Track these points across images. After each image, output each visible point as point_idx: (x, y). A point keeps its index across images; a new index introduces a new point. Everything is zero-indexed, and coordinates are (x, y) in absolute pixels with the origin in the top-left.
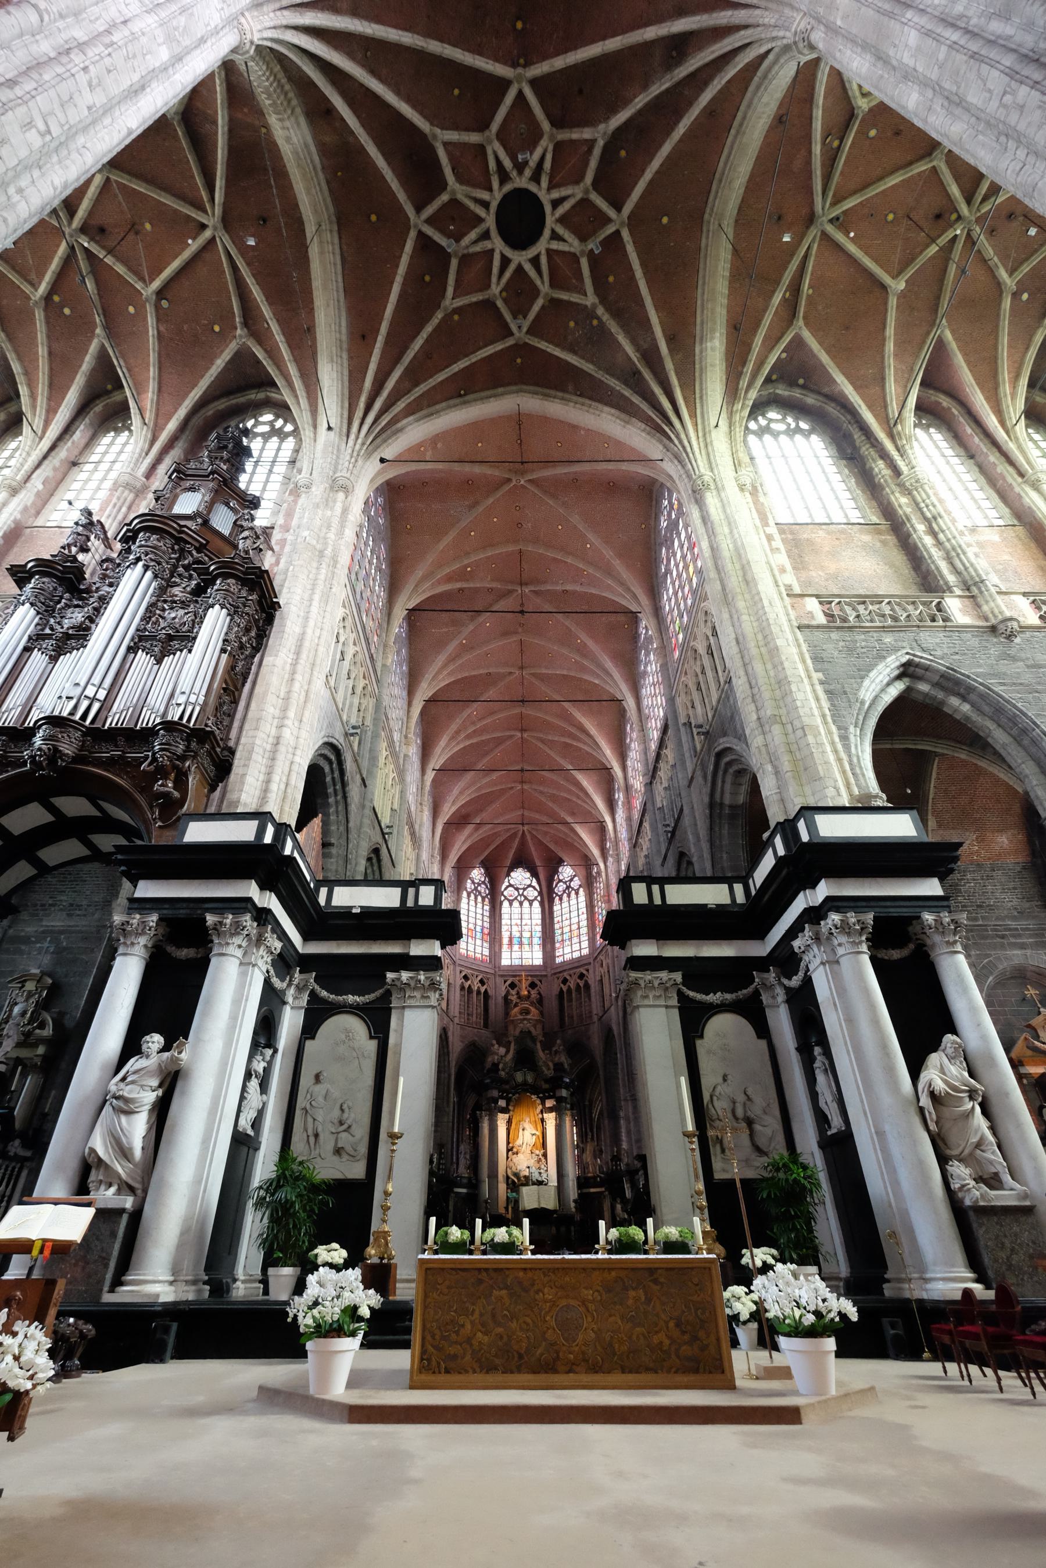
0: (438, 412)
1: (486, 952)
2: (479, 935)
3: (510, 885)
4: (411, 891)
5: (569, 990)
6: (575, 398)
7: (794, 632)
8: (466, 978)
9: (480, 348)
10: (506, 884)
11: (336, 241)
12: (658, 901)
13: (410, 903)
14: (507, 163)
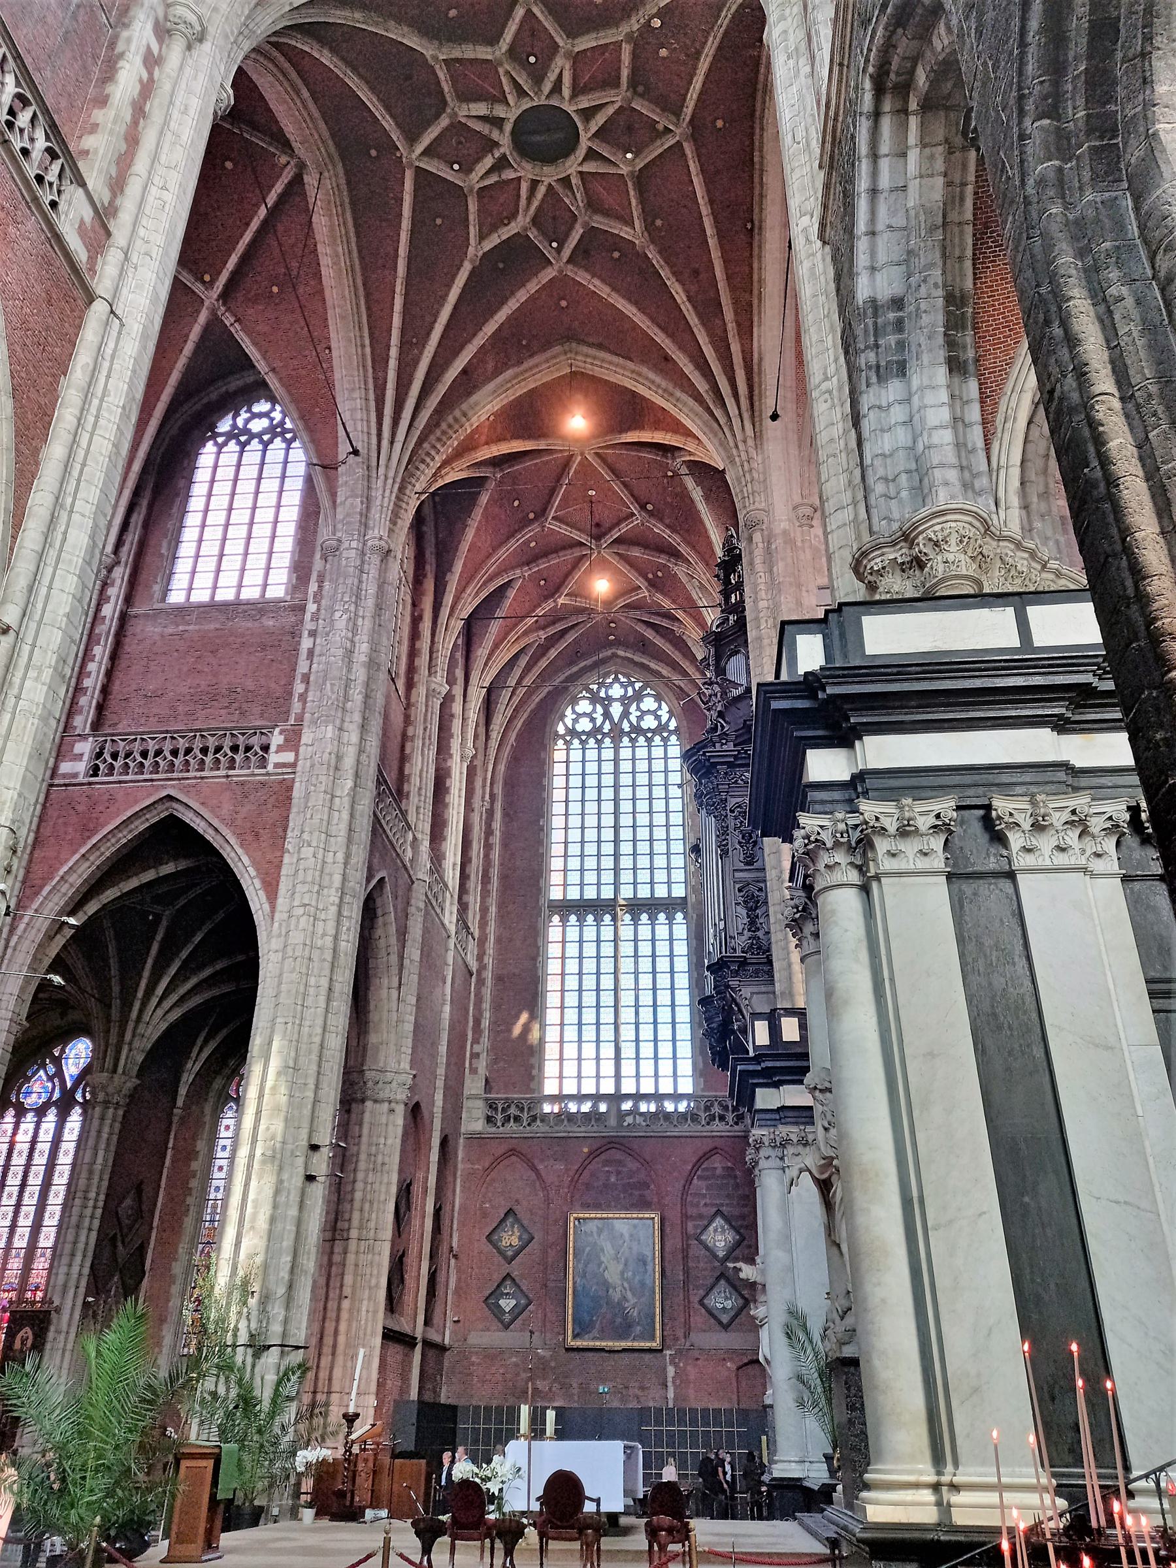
0: (760, 281)
11: (585, 349)
14: (488, 162)
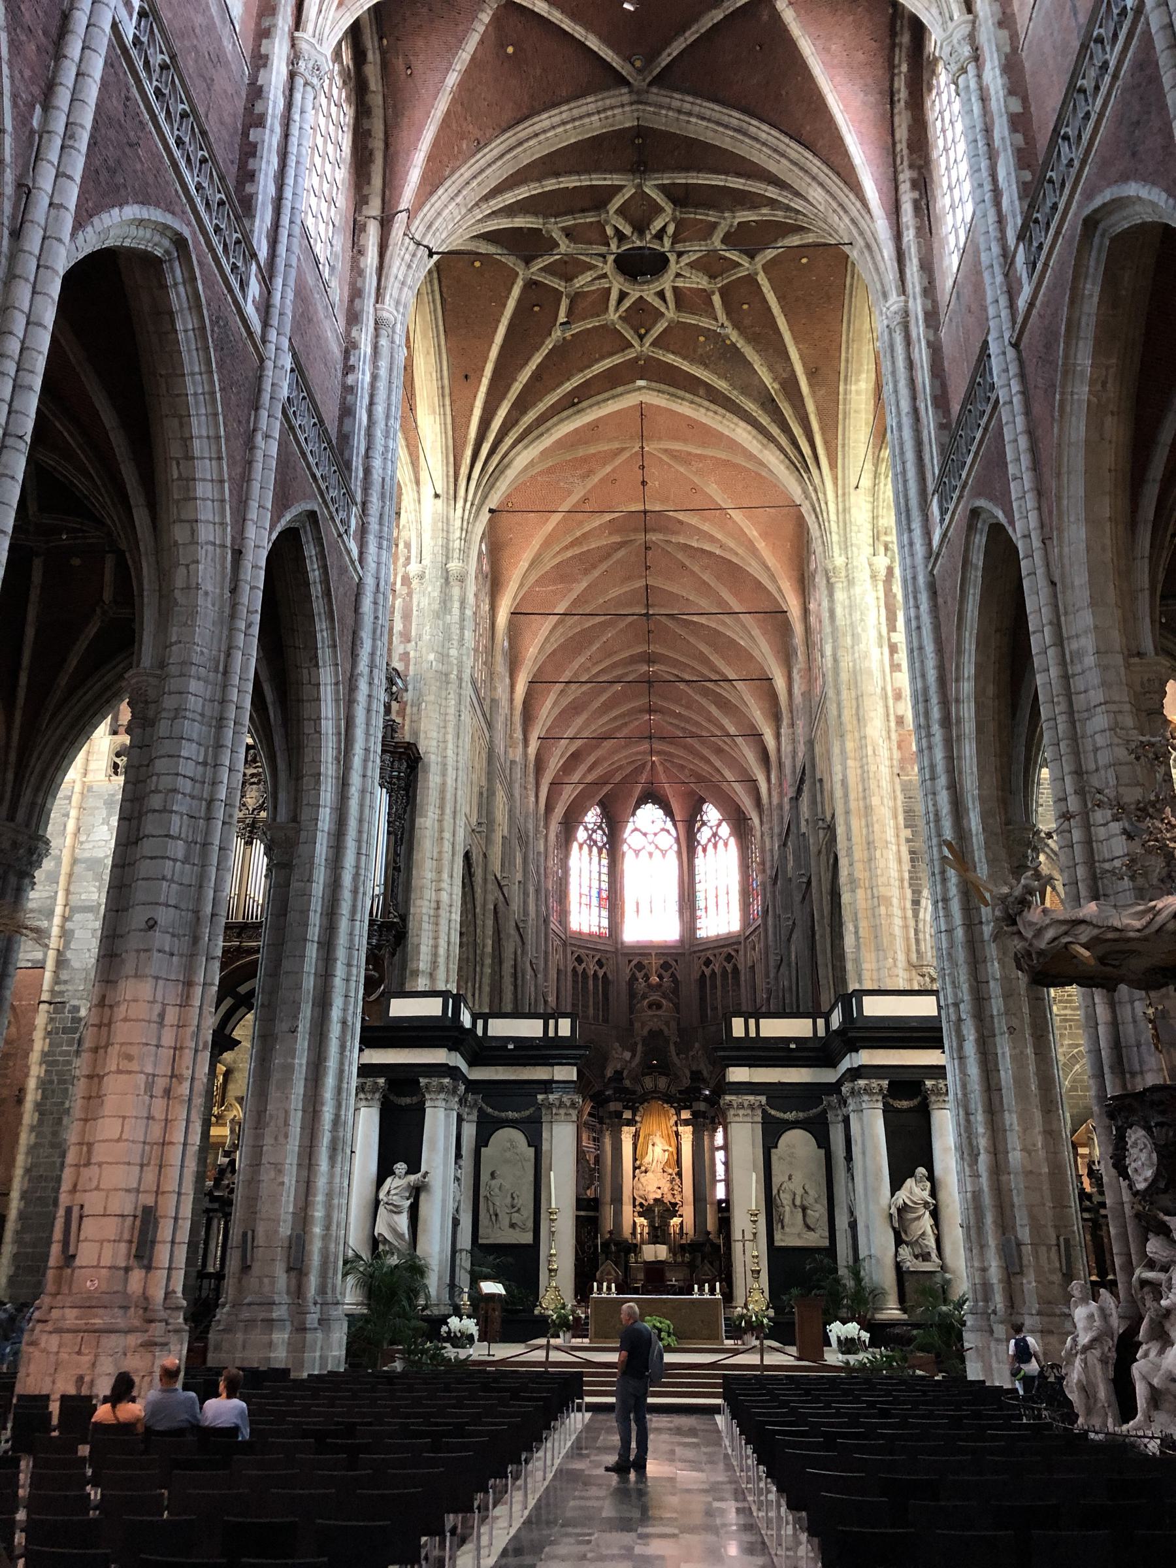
0: (548, 430)
1: (605, 923)
2: (595, 902)
3: (636, 829)
4: (552, 1022)
5: (713, 972)
6: (706, 403)
7: (892, 782)
8: (579, 960)
9: (597, 361)
10: (630, 827)
12: (753, 1034)
13: (551, 1034)
14: (627, 230)
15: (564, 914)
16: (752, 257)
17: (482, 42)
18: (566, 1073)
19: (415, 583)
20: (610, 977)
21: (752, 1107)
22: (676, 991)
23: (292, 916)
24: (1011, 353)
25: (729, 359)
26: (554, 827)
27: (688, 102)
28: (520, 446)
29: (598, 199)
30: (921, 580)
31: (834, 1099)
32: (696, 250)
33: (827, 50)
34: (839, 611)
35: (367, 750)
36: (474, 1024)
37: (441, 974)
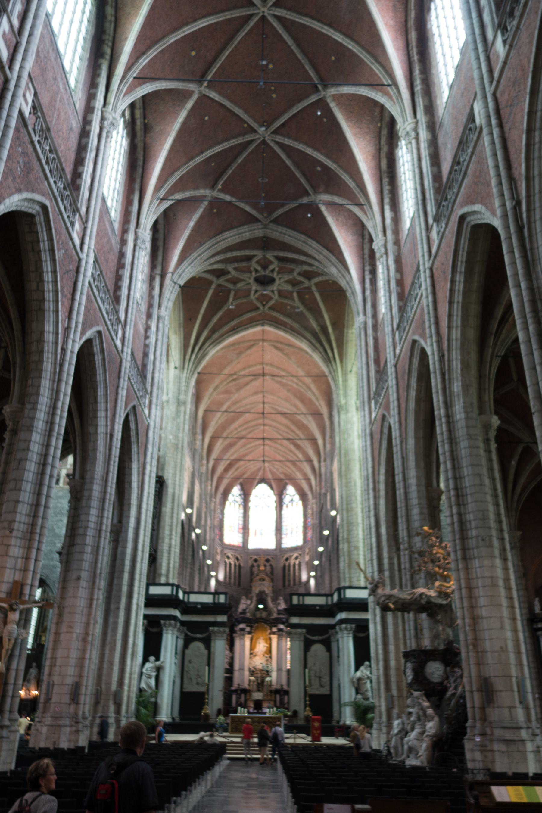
14: (259, 268)
15: (221, 535)
16: (309, 279)
17: (205, 210)
18: (222, 618)
19: (165, 404)
20: (242, 565)
21: (300, 634)
22: (272, 573)
23: (118, 562)
24: (393, 369)
25: (299, 317)
26: (219, 496)
27: (284, 230)
28: (211, 346)
29: (249, 258)
30: (368, 431)
31: (333, 631)
32: (287, 277)
33: (337, 220)
34: (342, 423)
35: (149, 493)
36: (184, 597)
37: (171, 575)
